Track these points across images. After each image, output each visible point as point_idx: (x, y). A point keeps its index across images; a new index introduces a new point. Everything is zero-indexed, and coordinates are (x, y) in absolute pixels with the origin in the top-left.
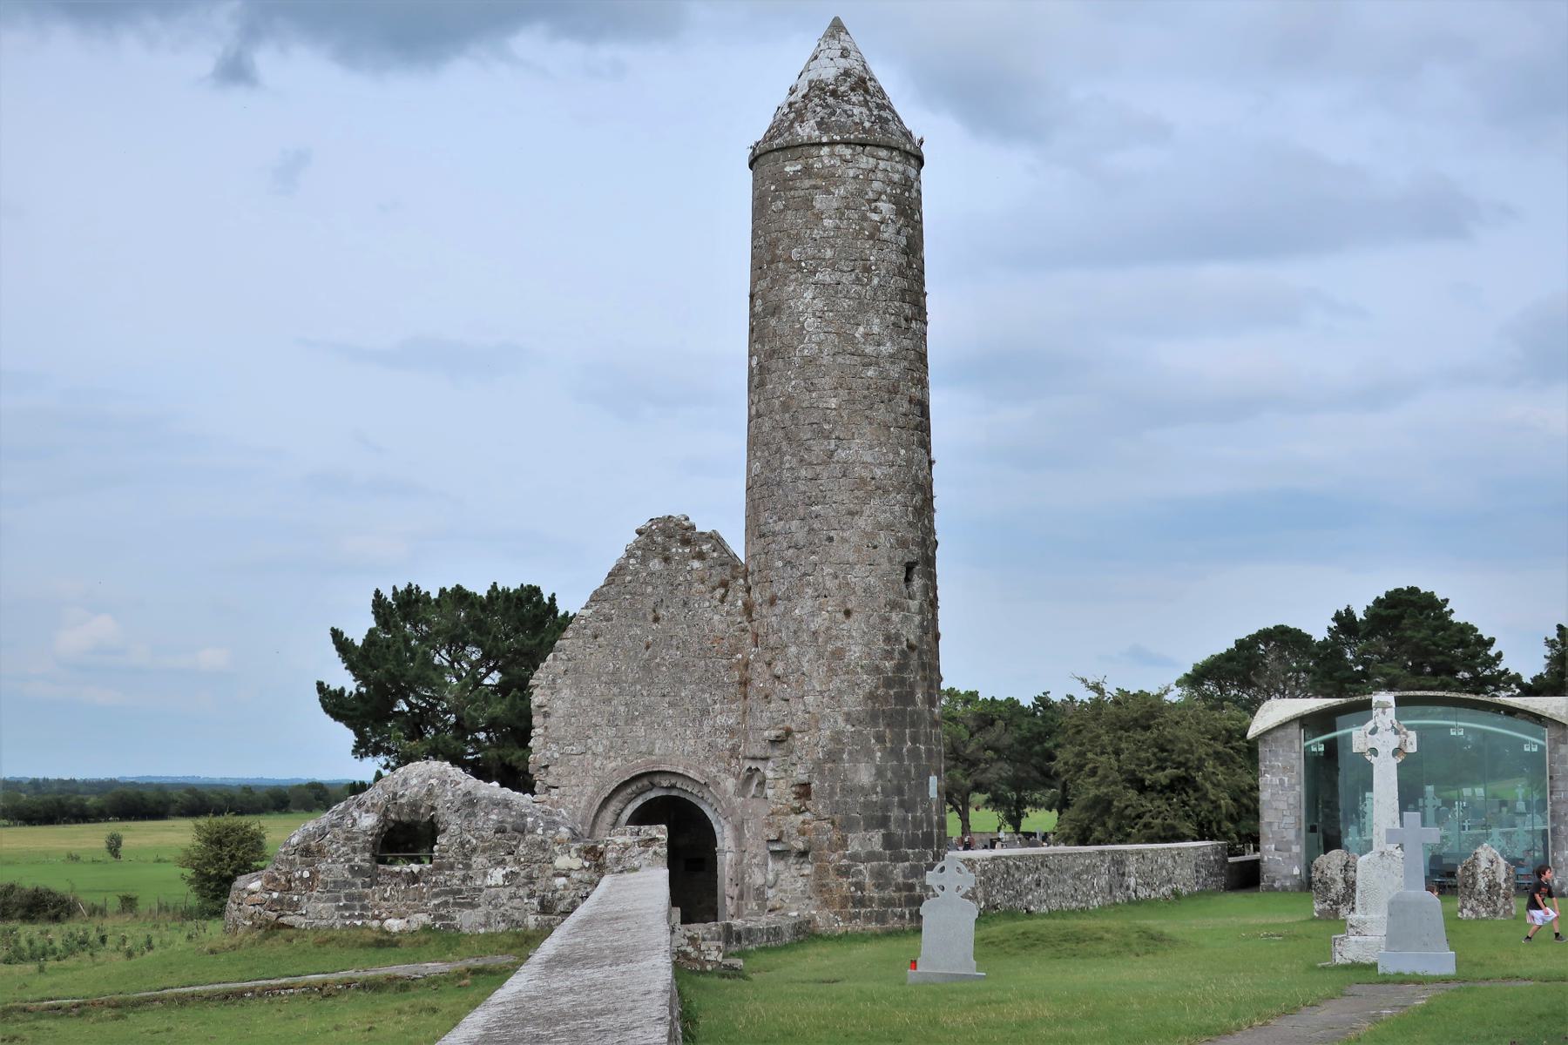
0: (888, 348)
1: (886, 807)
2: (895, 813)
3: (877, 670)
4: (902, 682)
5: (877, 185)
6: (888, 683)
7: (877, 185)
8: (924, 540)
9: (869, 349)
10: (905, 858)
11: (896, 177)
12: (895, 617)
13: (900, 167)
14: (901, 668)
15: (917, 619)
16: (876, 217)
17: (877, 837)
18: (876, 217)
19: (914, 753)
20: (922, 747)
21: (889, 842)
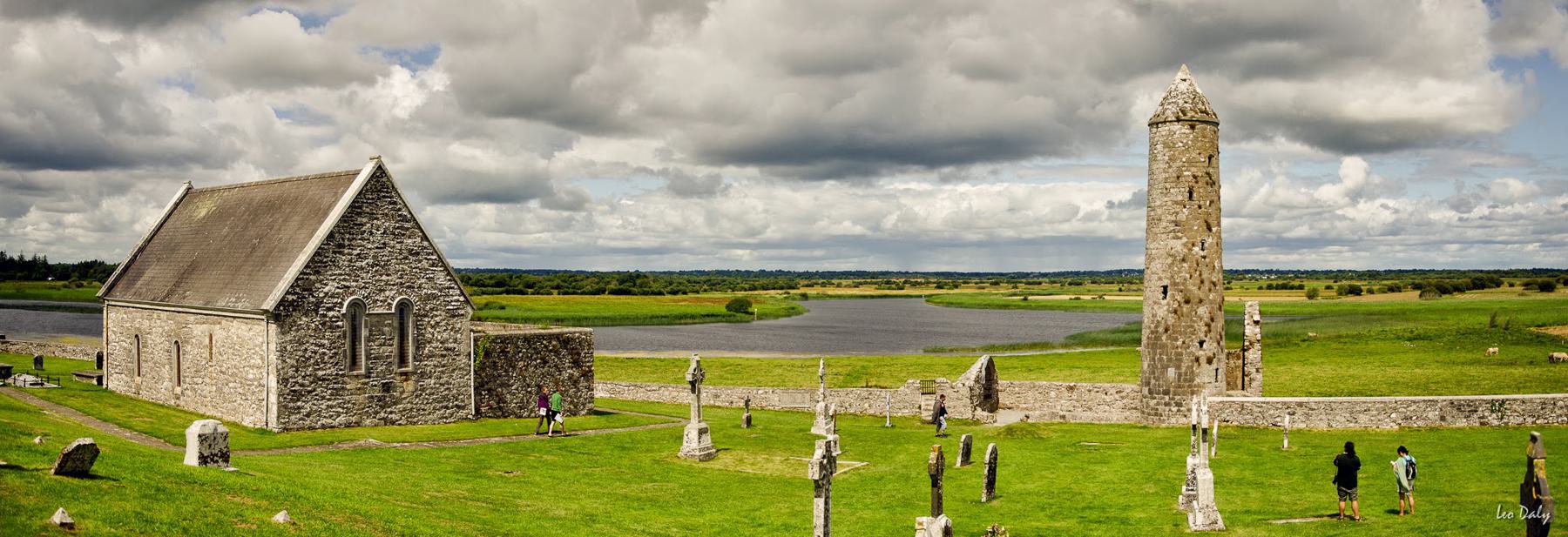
0: (1158, 203)
1: (1150, 378)
2: (1153, 381)
3: (1150, 327)
4: (1157, 332)
5: (1156, 139)
6: (1152, 332)
7: (1156, 139)
8: (1172, 277)
9: (1153, 204)
10: (1155, 398)
11: (1164, 133)
12: (1156, 307)
13: (1167, 128)
14: (1156, 327)
15: (1165, 308)
16: (1155, 151)
17: (1147, 389)
18: (1155, 151)
19: (1161, 360)
20: (1165, 357)
21: (1150, 392)
